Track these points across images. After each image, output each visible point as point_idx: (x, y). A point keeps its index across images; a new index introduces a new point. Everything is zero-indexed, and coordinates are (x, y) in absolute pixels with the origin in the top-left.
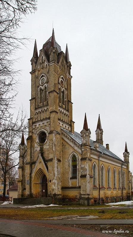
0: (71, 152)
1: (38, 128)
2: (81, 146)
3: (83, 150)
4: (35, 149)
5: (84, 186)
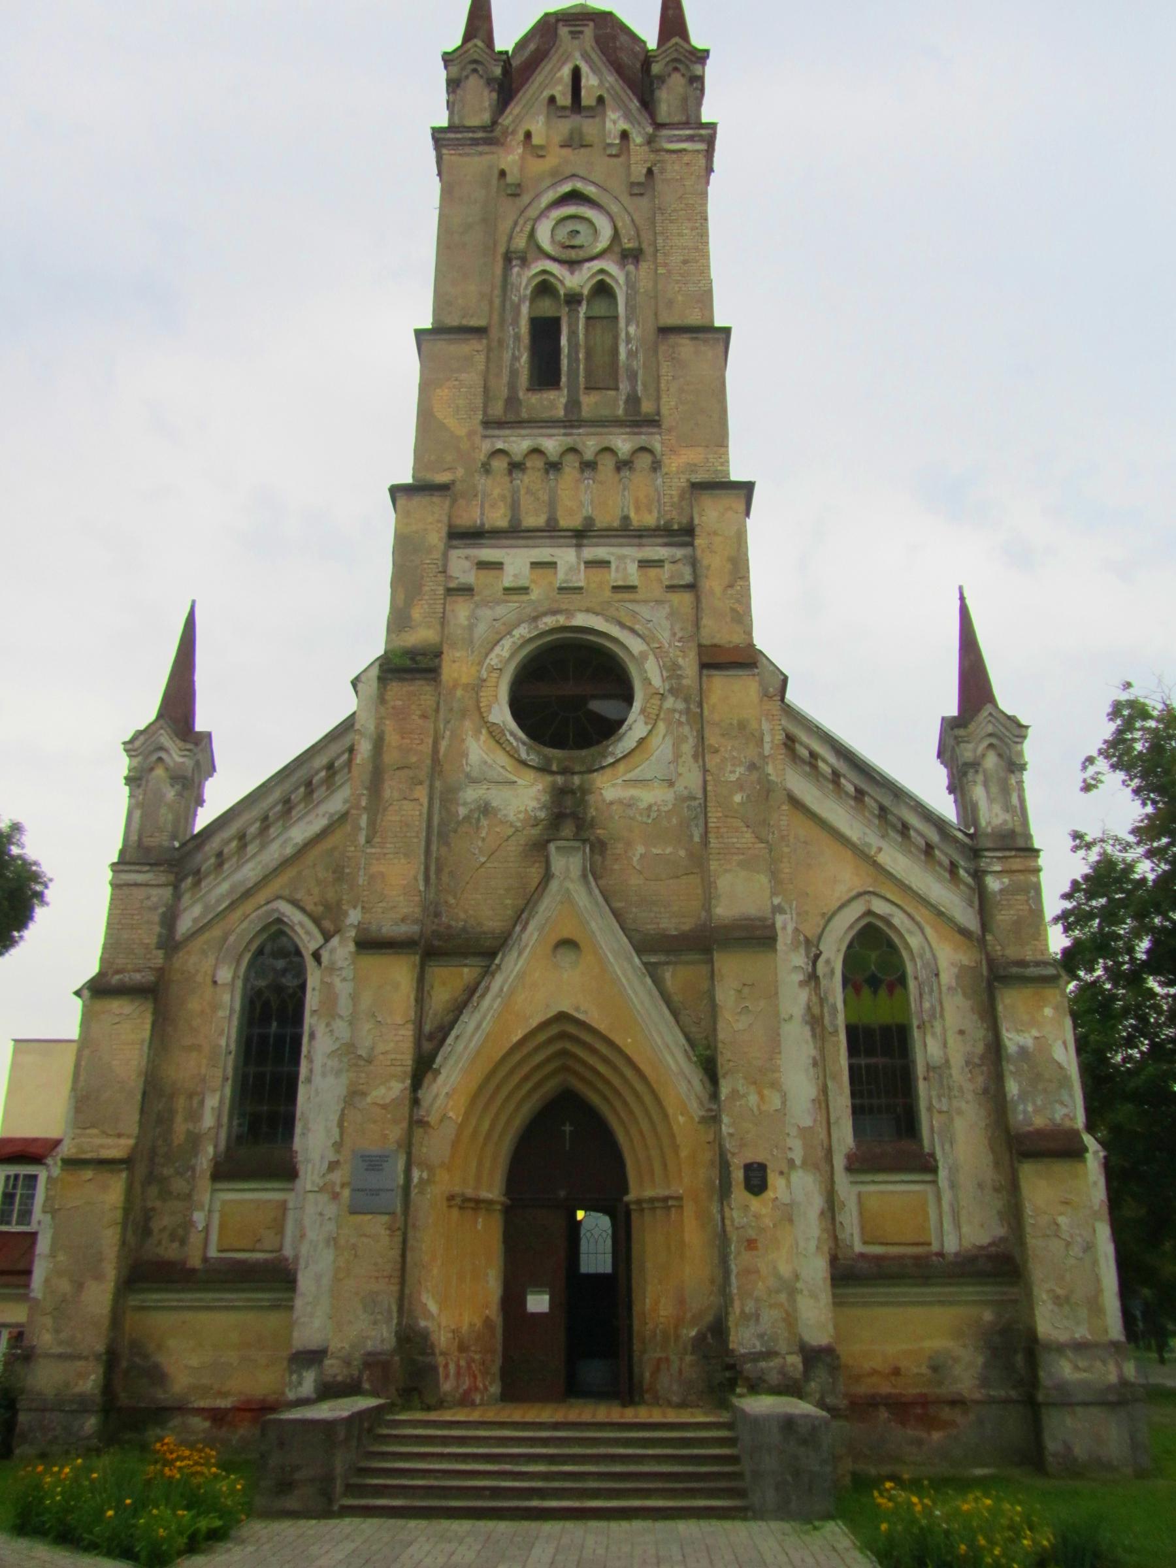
0: (842, 891)
1: (524, 590)
2: (975, 853)
3: (993, 884)
4: (471, 795)
5: (1076, 1250)
